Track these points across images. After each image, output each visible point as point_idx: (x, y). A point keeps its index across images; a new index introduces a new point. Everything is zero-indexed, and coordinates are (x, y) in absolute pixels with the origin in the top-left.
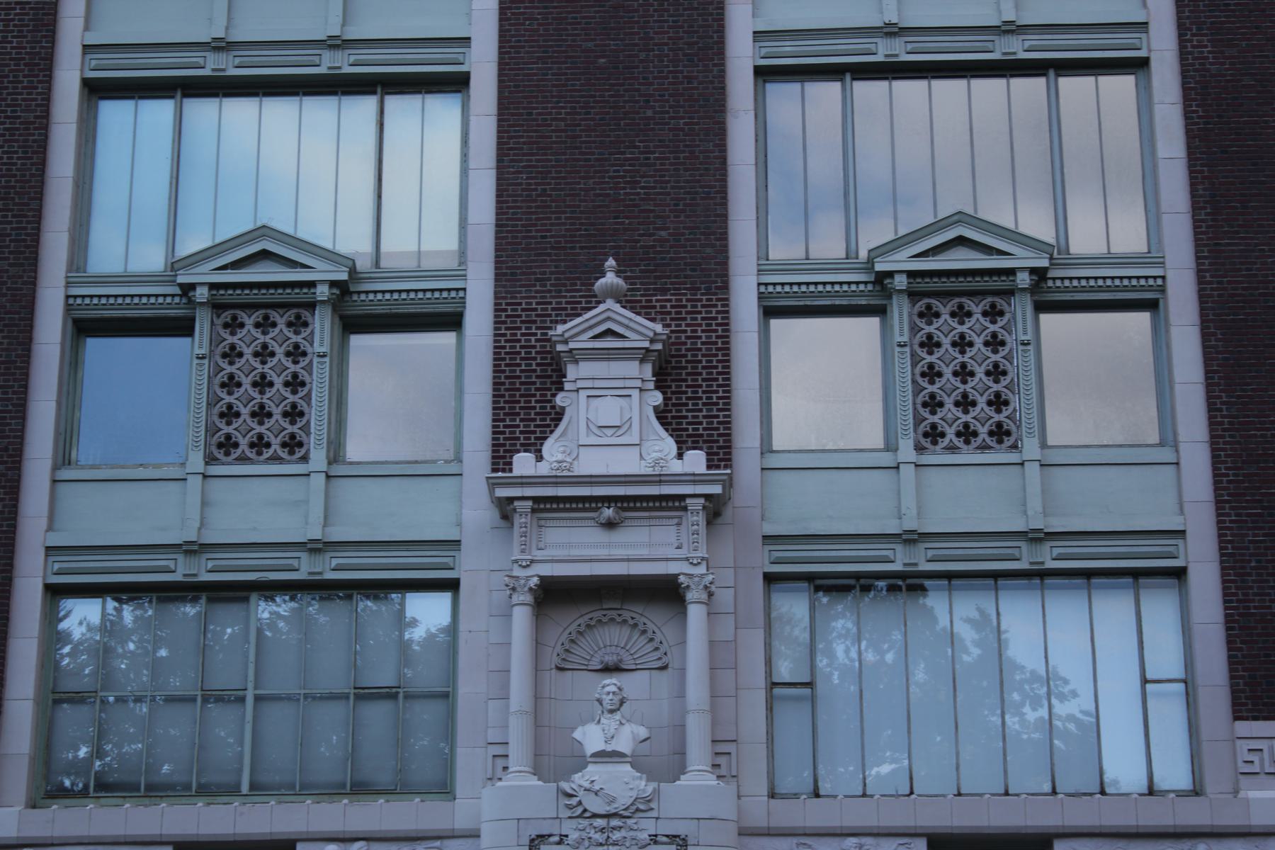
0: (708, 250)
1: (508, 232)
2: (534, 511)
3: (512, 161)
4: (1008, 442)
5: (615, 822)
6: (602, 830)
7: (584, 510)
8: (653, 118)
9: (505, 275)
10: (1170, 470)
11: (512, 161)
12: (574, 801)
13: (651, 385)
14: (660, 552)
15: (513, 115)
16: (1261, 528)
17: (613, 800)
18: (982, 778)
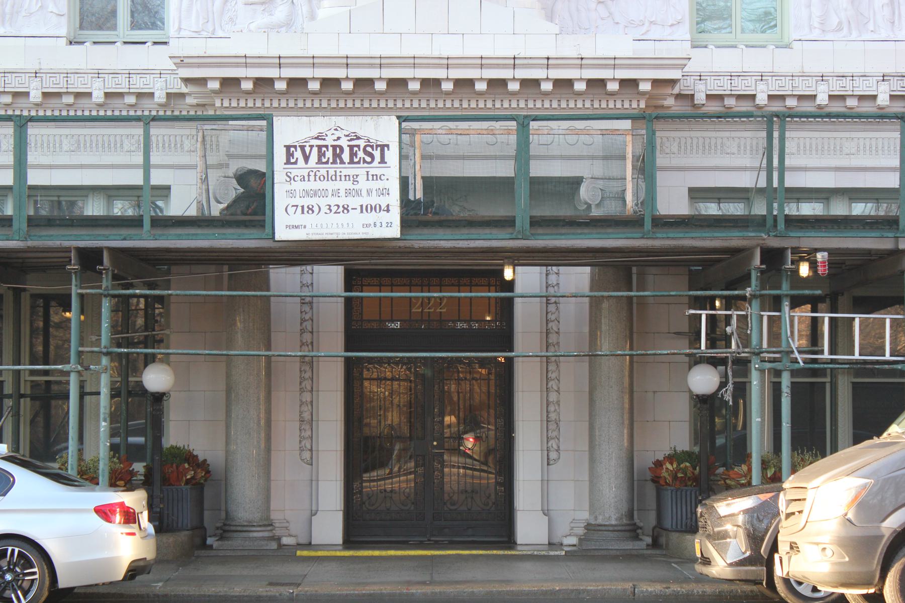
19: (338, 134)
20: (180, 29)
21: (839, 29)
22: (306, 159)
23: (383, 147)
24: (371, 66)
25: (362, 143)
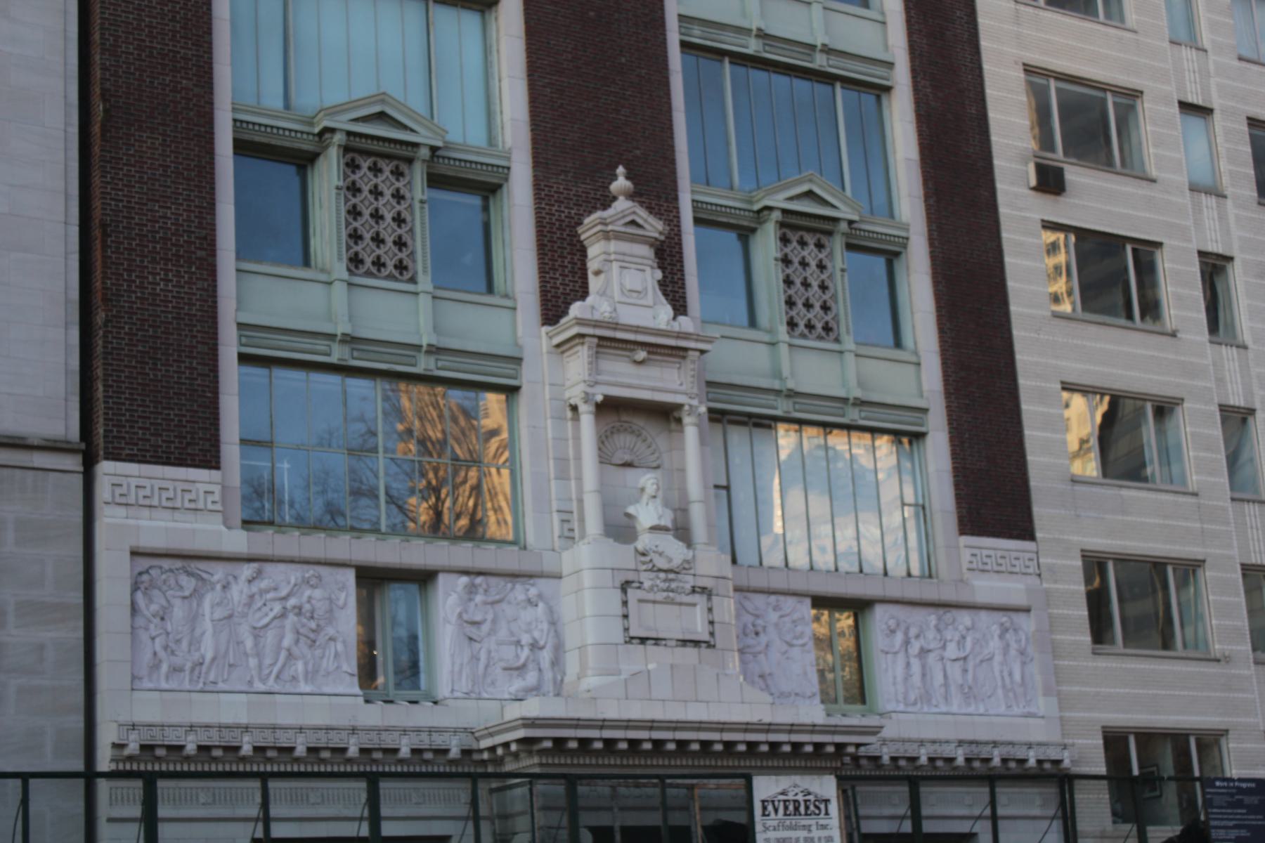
2: (599, 346)
4: (832, 336)
5: (671, 576)
6: (665, 581)
7: (625, 349)
10: (911, 368)
12: (647, 559)
17: (670, 560)
18: (824, 560)
19: (796, 790)
20: (453, 690)
21: (915, 703)
22: (776, 811)
23: (827, 801)
24: (668, 729)
25: (811, 798)
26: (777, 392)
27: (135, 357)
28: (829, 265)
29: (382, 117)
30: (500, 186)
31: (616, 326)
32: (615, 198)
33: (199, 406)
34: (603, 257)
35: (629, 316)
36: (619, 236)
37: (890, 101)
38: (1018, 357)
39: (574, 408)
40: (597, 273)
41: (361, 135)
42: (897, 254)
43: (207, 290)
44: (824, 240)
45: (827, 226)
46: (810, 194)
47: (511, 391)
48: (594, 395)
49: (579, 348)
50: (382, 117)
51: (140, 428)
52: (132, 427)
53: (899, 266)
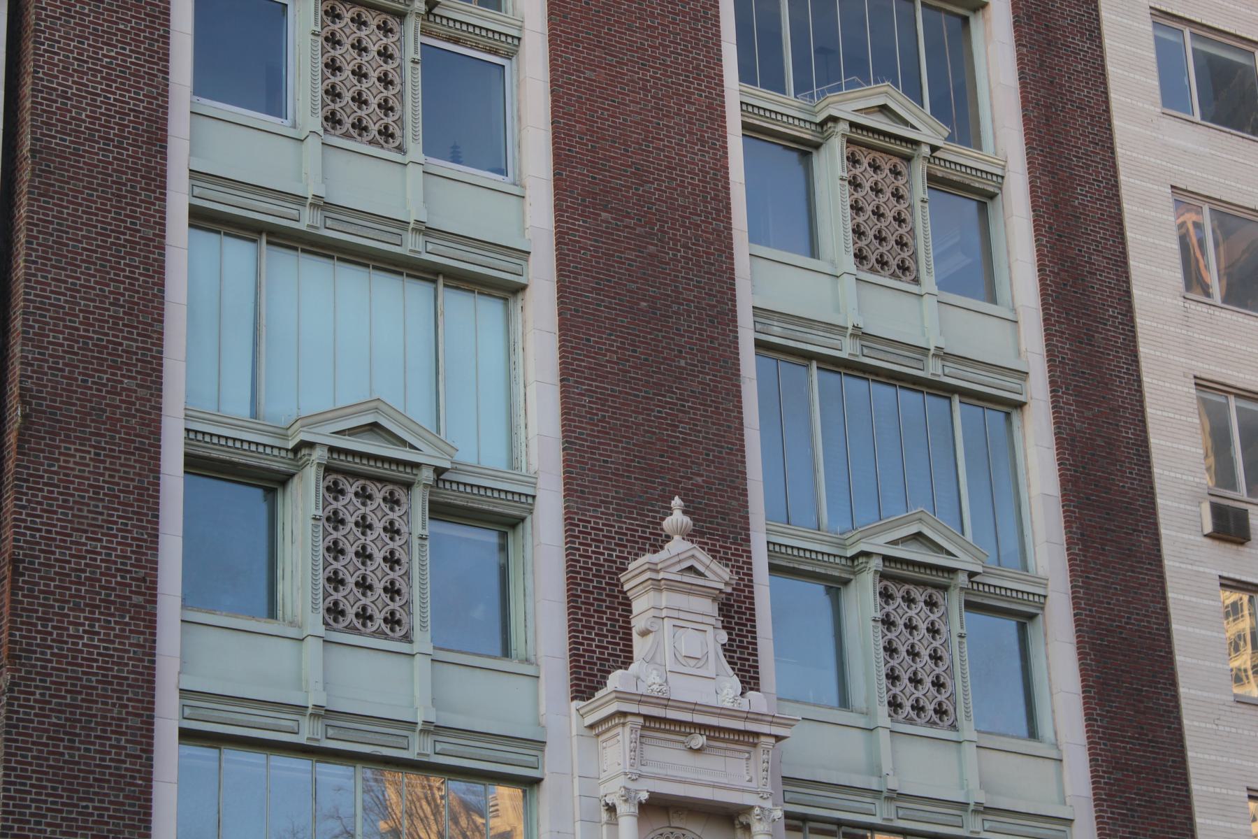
0: (734, 503)
1: (576, 450)
2: (644, 727)
3: (576, 382)
4: (947, 721)
7: (679, 733)
8: (685, 368)
9: (571, 490)
11: (576, 382)
13: (720, 625)
14: (736, 782)
15: (575, 337)
16: (1127, 827)
26: (876, 793)
27: (47, 731)
28: (943, 629)
29: (374, 428)
30: (523, 519)
31: (667, 703)
32: (669, 538)
33: (126, 797)
34: (652, 613)
35: (684, 690)
36: (673, 586)
37: (1023, 421)
38: (1190, 754)
39: (611, 809)
40: (644, 633)
41: (347, 452)
42: (1032, 617)
43: (143, 646)
44: (937, 596)
45: (940, 579)
46: (918, 537)
47: (530, 784)
48: (637, 791)
49: (619, 729)
50: (374, 428)
51: (48, 825)
52: (38, 823)
53: (1034, 631)
